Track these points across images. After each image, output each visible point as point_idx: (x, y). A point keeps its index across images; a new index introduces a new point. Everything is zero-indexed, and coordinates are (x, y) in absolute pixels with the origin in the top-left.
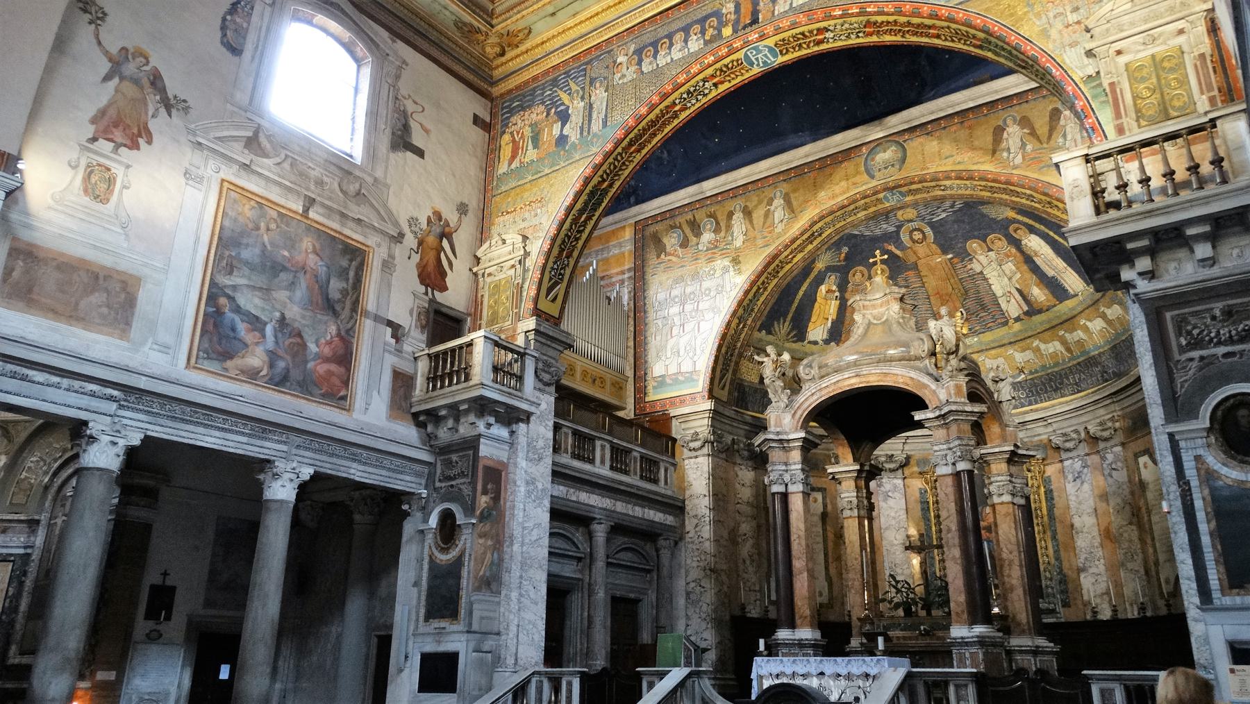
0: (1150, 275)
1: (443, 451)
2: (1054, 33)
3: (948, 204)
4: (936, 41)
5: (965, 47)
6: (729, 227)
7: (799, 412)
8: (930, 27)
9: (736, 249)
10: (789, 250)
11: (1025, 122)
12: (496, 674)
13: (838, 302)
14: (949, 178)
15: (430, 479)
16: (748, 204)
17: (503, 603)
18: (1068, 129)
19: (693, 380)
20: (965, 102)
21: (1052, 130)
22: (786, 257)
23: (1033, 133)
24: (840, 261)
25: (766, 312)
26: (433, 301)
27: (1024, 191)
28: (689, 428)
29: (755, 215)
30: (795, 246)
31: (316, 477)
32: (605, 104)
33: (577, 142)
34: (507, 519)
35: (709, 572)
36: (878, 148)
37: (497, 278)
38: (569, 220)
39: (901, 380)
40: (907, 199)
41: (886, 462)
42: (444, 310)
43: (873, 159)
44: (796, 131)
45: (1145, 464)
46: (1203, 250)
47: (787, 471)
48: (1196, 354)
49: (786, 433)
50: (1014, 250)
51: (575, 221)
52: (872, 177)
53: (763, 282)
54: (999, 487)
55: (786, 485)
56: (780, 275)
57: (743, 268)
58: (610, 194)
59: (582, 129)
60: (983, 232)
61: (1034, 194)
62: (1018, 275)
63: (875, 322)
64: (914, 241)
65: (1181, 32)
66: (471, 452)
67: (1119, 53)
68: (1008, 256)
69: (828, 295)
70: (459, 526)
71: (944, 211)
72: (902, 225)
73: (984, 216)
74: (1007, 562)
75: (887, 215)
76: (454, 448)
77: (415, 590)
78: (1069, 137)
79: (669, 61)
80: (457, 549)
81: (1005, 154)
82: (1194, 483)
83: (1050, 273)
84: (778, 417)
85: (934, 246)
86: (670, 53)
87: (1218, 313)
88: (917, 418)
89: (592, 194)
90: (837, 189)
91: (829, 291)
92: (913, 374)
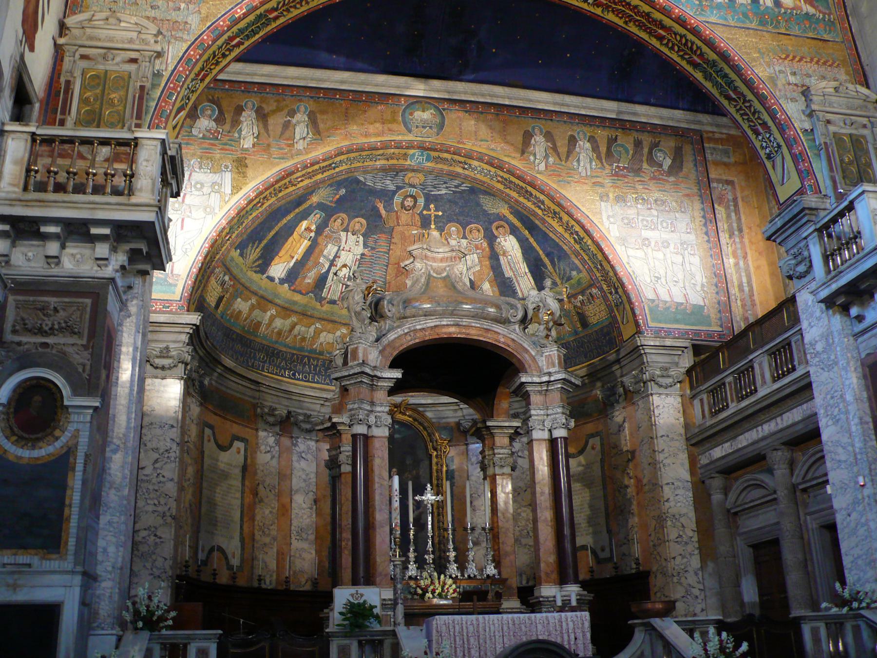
2: (779, 83)
3: (456, 182)
4: (654, 42)
5: (678, 60)
6: (236, 123)
7: (388, 350)
8: (663, 27)
9: (243, 149)
10: (304, 172)
11: (549, 136)
12: (91, 637)
13: (310, 243)
14: (481, 160)
16: (264, 106)
17: (102, 533)
18: (581, 157)
20: (503, 97)
21: (569, 153)
22: (297, 178)
23: (555, 149)
24: (331, 202)
25: (249, 231)
26: (22, 56)
27: (538, 195)
28: (156, 341)
29: (271, 121)
30: (310, 170)
35: (169, 520)
36: (417, 106)
37: (101, 67)
38: (225, 37)
39: (502, 340)
40: (429, 164)
41: (303, 421)
42: (26, 79)
43: (411, 114)
44: (331, 51)
47: (372, 411)
49: (382, 369)
50: (485, 245)
51: (231, 39)
52: (410, 131)
53: (264, 198)
54: (501, 459)
55: (369, 427)
56: (280, 195)
57: (250, 173)
58: (269, 28)
60: (468, 219)
61: (547, 201)
62: (478, 268)
63: (435, 275)
64: (403, 206)
65: (865, 126)
66: (88, 301)
67: (828, 122)
68: (477, 248)
69: (306, 234)
70: (67, 407)
71: (447, 188)
72: (403, 187)
73: (478, 204)
74: (503, 530)
75: (396, 171)
76: (47, 288)
78: (582, 164)
80: (58, 444)
81: (532, 158)
83: (508, 273)
84: (365, 350)
85: (417, 218)
88: (523, 380)
89: (260, 17)
90: (371, 129)
91: (308, 229)
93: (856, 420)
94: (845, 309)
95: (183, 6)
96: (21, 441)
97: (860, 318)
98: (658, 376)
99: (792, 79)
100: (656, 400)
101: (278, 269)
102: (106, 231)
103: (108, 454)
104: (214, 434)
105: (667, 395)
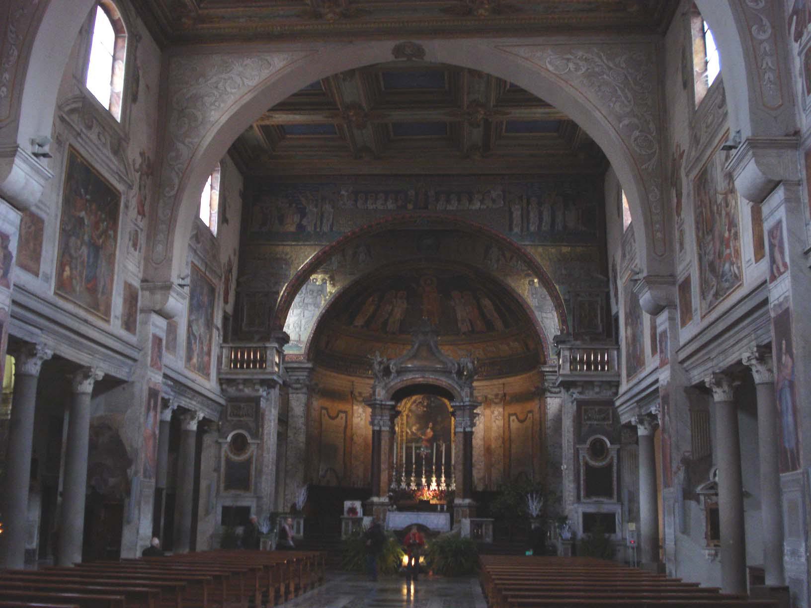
0: (580, 393)
1: (230, 399)
15: (223, 413)
19: (297, 346)
31: (204, 418)
32: (331, 217)
33: (312, 232)
34: (265, 440)
45: (513, 420)
46: (597, 389)
48: (589, 422)
55: (380, 427)
59: (315, 225)
66: (254, 404)
77: (215, 474)
79: (375, 208)
81: (489, 262)
82: (582, 464)
86: (376, 204)
87: (597, 410)
92: (450, 382)
93: (566, 441)
94: (568, 391)
95: (284, 266)
96: (235, 454)
97: (572, 396)
98: (551, 387)
99: (564, 272)
100: (549, 400)
101: (359, 322)
102: (258, 381)
103: (264, 455)
104: (327, 411)
105: (555, 397)
